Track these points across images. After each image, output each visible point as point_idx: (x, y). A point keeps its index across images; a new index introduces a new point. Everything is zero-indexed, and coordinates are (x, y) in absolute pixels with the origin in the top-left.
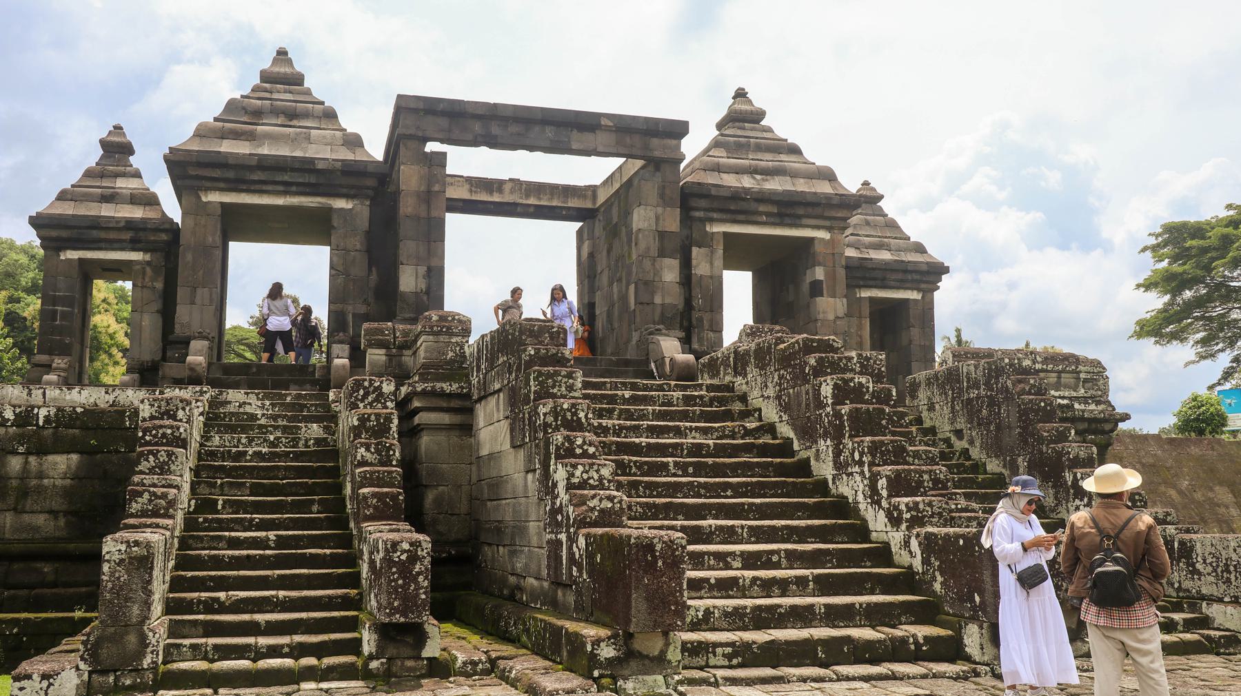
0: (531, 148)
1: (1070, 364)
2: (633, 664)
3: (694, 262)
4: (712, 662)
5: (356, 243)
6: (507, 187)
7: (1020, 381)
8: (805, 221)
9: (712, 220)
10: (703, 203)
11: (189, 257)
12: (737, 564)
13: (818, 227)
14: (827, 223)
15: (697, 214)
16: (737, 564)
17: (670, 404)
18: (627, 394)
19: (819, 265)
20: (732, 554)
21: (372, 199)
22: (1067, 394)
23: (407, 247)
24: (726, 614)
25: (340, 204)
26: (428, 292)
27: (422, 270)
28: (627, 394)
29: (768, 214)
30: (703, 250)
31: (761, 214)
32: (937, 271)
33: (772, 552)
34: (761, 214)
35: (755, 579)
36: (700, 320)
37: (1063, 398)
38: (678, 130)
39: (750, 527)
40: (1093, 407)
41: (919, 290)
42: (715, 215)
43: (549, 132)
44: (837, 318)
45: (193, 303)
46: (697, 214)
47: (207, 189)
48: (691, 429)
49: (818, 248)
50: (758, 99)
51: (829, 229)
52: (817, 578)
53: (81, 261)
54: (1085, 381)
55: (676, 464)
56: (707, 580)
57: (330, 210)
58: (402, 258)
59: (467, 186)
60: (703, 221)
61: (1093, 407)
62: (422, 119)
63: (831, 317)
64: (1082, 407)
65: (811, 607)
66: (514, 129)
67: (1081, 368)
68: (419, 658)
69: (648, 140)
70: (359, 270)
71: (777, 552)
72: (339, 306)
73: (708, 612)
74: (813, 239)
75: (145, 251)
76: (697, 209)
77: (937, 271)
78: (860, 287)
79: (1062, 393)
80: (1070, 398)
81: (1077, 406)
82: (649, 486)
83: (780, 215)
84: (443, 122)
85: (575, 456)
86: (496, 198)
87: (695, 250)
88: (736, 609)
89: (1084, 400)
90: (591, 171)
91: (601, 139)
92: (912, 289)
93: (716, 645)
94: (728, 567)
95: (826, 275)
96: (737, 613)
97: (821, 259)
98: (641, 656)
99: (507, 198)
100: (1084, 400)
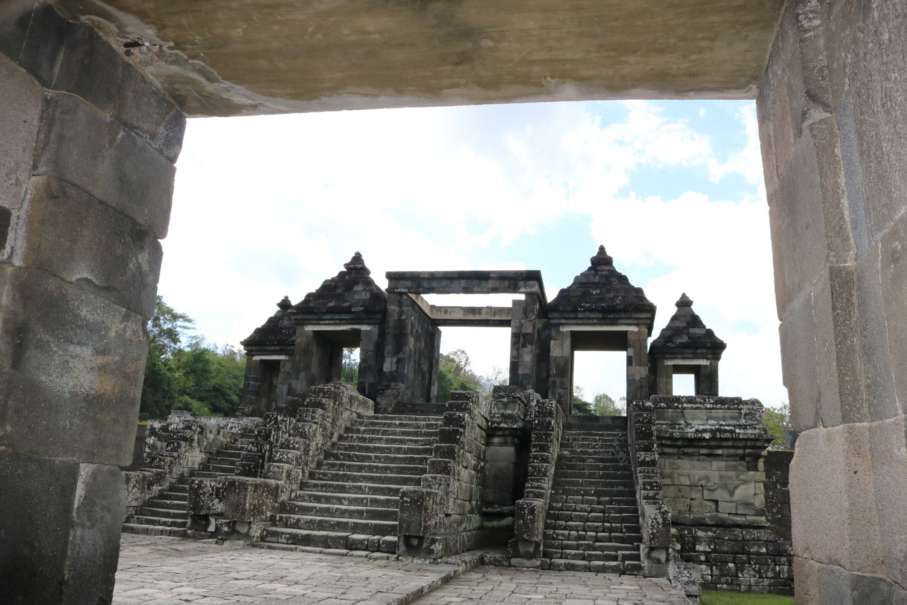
0: (458, 292)
1: (734, 404)
2: (235, 535)
3: (551, 349)
4: (280, 540)
5: (371, 347)
6: (483, 311)
7: (639, 415)
9: (563, 324)
10: (556, 315)
11: (298, 357)
12: (346, 503)
13: (630, 324)
14: (635, 322)
15: (553, 321)
16: (346, 503)
17: (419, 427)
18: (397, 422)
20: (344, 498)
21: (380, 324)
22: (732, 422)
23: (389, 348)
24: (307, 522)
25: (364, 328)
26: (397, 371)
27: (395, 360)
28: (397, 422)
29: (596, 318)
30: (557, 342)
31: (593, 319)
32: (721, 346)
33: (363, 499)
34: (593, 319)
35: (337, 509)
36: (554, 383)
37: (729, 425)
38: (534, 277)
39: (369, 487)
40: (750, 431)
41: (708, 359)
42: (563, 321)
43: (463, 283)
45: (298, 379)
46: (553, 321)
48: (408, 440)
49: (630, 337)
50: (609, 253)
51: (637, 325)
52: (368, 512)
53: (261, 360)
54: (746, 414)
55: (376, 457)
56: (315, 508)
57: (359, 331)
58: (386, 355)
59: (462, 312)
60: (559, 325)
61: (750, 431)
63: (637, 378)
64: (742, 431)
65: (347, 523)
66: (444, 283)
67: (741, 406)
68: (206, 531)
70: (371, 362)
71: (367, 499)
72: (361, 380)
73: (298, 520)
74: (626, 333)
75: (286, 355)
77: (721, 346)
78: (667, 359)
79: (727, 423)
80: (734, 426)
81: (738, 431)
82: (349, 466)
83: (604, 318)
84: (409, 283)
85: (289, 448)
86: (478, 317)
87: (552, 343)
88: (311, 520)
89: (745, 427)
90: (504, 300)
91: (491, 284)
92: (703, 358)
93: (283, 533)
94: (341, 504)
95: (635, 352)
96: (311, 521)
97: (631, 343)
98: (238, 532)
99: (483, 317)
100: (745, 427)
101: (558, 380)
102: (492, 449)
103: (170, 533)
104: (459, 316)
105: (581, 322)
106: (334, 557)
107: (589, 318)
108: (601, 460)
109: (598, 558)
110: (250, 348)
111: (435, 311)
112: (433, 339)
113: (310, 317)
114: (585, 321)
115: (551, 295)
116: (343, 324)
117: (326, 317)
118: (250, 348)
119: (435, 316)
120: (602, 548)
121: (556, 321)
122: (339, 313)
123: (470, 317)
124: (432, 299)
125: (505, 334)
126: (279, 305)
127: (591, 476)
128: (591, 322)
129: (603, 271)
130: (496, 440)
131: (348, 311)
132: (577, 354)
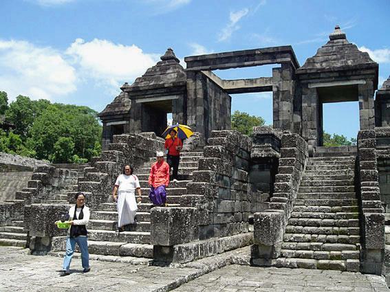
8: (352, 77)
13: (360, 79)
14: (363, 77)
19: (360, 95)
27: (194, 117)
29: (335, 77)
31: (332, 77)
34: (332, 77)
38: (288, 51)
42: (311, 81)
44: (370, 118)
46: (303, 82)
47: (138, 99)
51: (365, 79)
58: (188, 114)
60: (307, 84)
62: (201, 64)
69: (281, 55)
76: (304, 80)
101: (309, 123)
102: (253, 173)
103: (18, 245)
104: (241, 85)
105: (323, 80)
106: (102, 264)
107: (330, 77)
108: (335, 178)
109: (326, 257)
110: (104, 118)
111: (225, 84)
112: (225, 108)
113: (139, 93)
114: (327, 80)
115: (301, 62)
116: (160, 96)
117: (148, 93)
118: (104, 118)
119: (226, 87)
120: (329, 249)
121: (305, 81)
122: (157, 89)
123: (250, 86)
124: (223, 76)
125: (268, 96)
126: (121, 89)
127: (326, 190)
128: (331, 80)
129: (338, 42)
130: (256, 167)
131: (162, 87)
132: (324, 105)
